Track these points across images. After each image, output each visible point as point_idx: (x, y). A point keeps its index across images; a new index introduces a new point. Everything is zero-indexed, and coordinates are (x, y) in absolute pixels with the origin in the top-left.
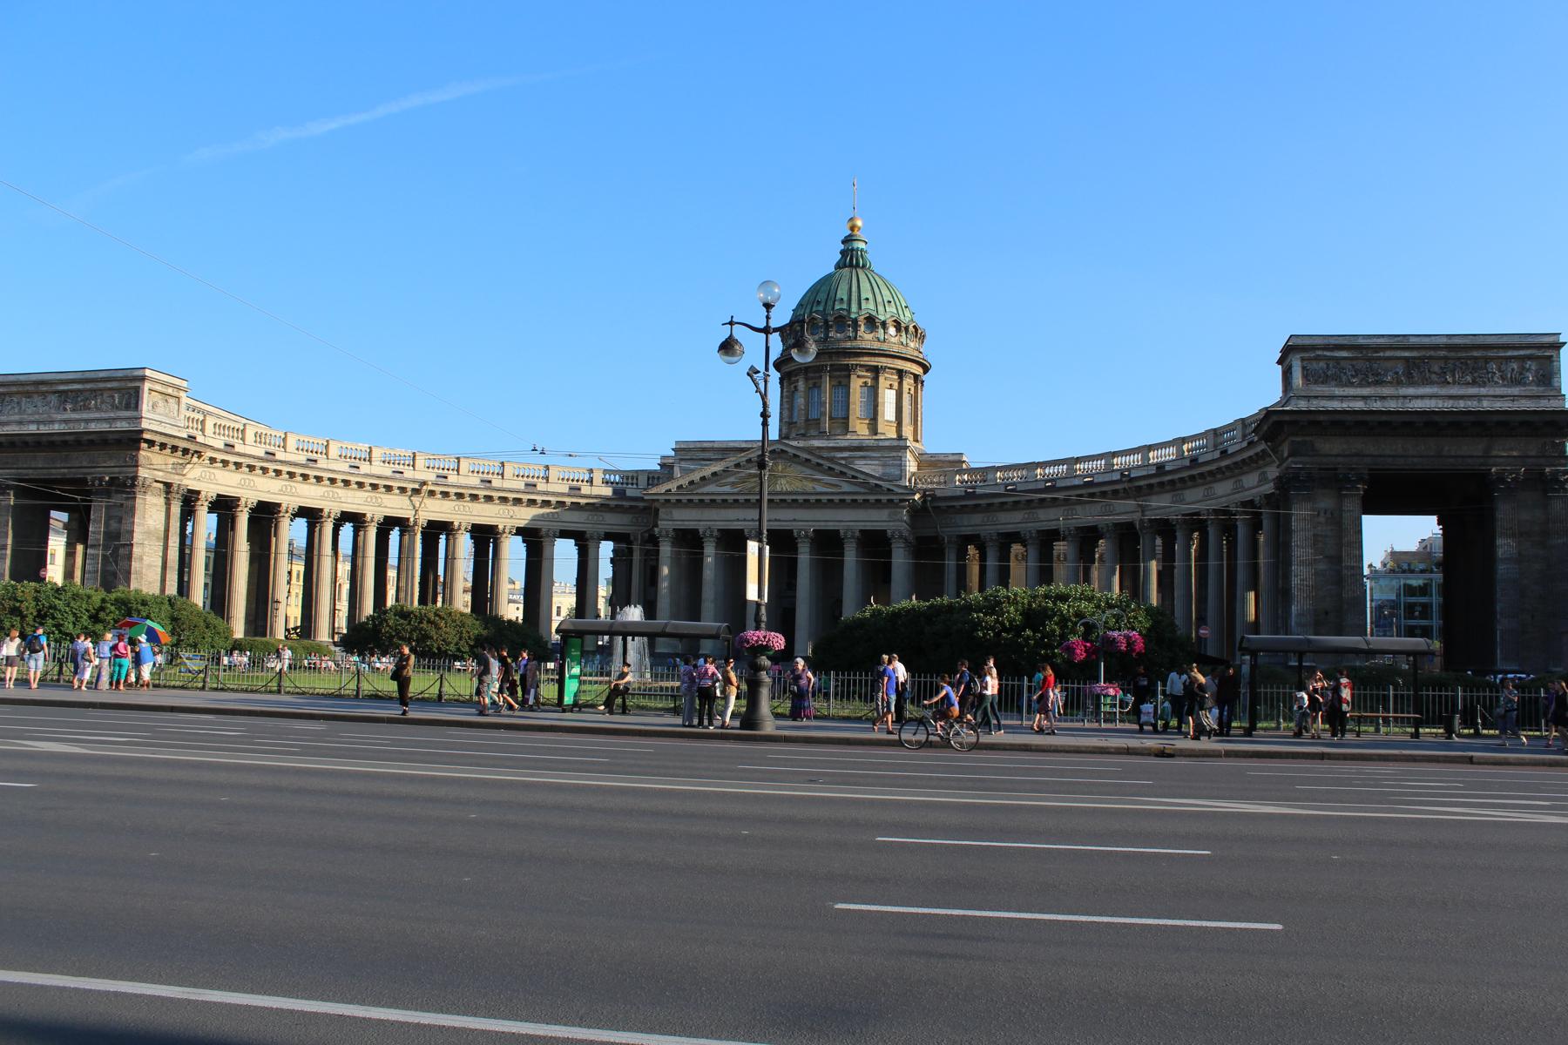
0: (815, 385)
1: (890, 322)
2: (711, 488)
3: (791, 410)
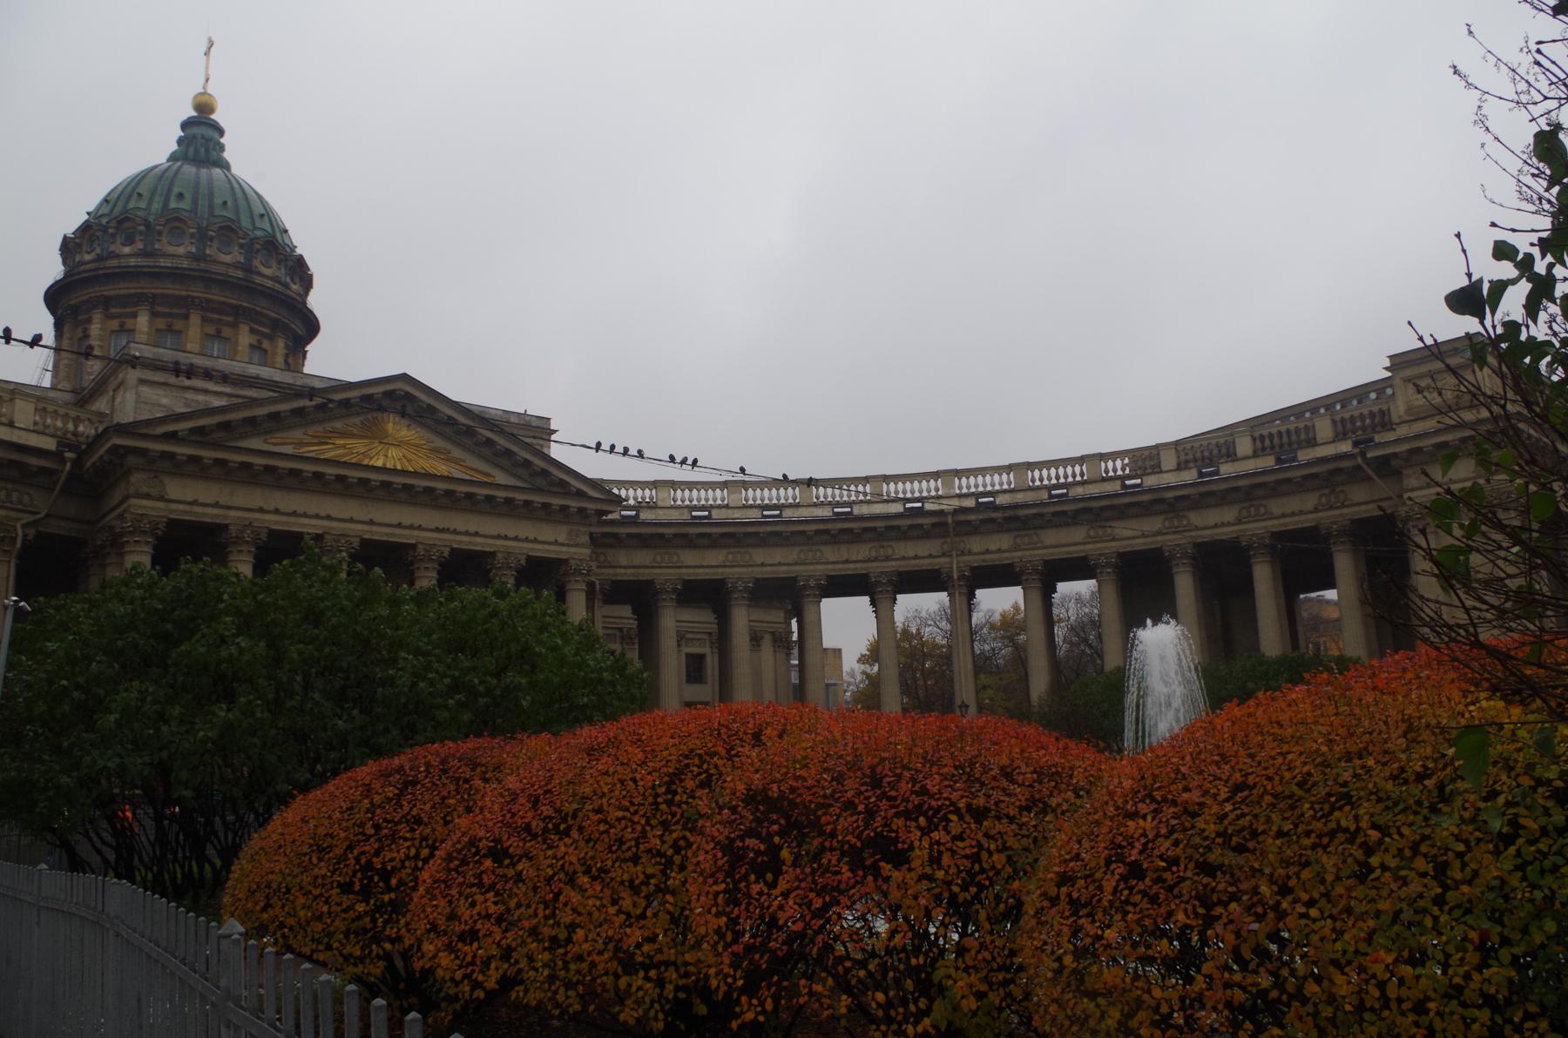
0: (170, 329)
2: (256, 443)
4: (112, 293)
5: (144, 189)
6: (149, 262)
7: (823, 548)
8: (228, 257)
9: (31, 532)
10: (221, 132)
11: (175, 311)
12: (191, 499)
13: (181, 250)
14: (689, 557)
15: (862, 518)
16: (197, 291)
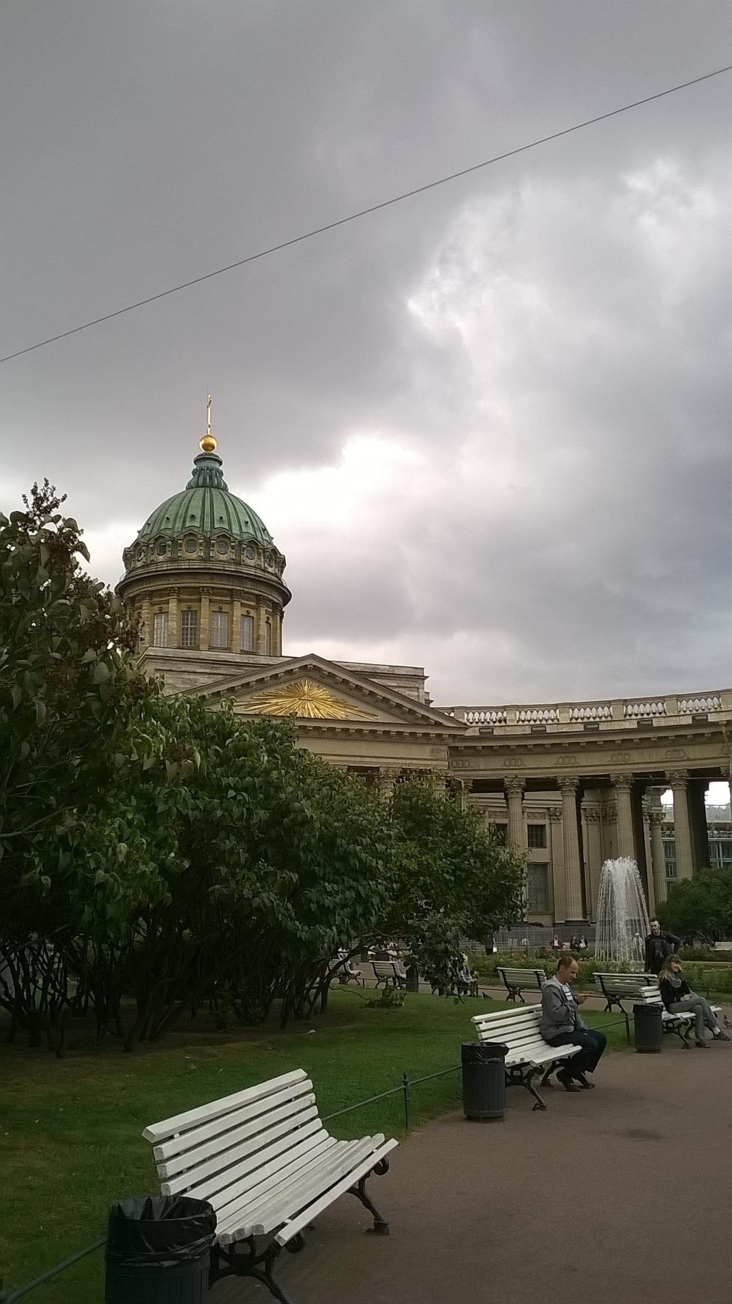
4: (153, 588)
5: (171, 514)
6: (174, 566)
7: (630, 752)
8: (223, 557)
10: (221, 463)
11: (193, 597)
13: (194, 555)
15: (659, 729)
16: (205, 583)
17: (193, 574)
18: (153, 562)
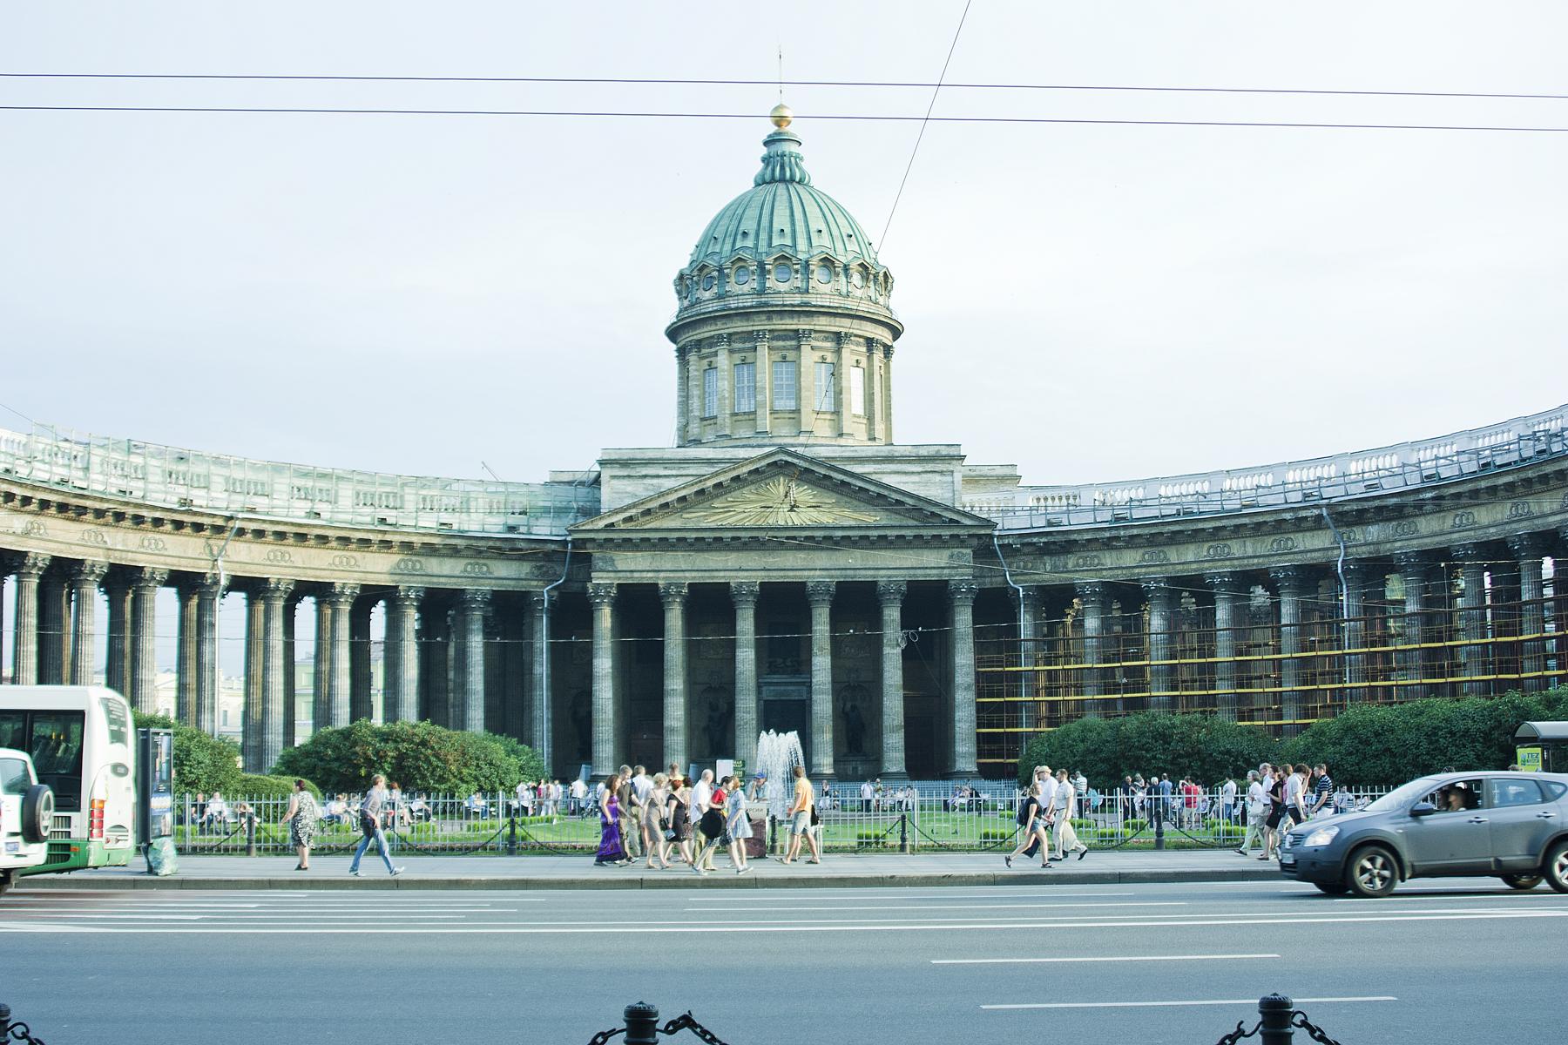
1: (854, 265)
3: (703, 397)
9: (555, 593)
12: (636, 567)
13: (746, 288)
14: (1109, 559)
16: (759, 324)
17: (745, 314)
18: (699, 301)
